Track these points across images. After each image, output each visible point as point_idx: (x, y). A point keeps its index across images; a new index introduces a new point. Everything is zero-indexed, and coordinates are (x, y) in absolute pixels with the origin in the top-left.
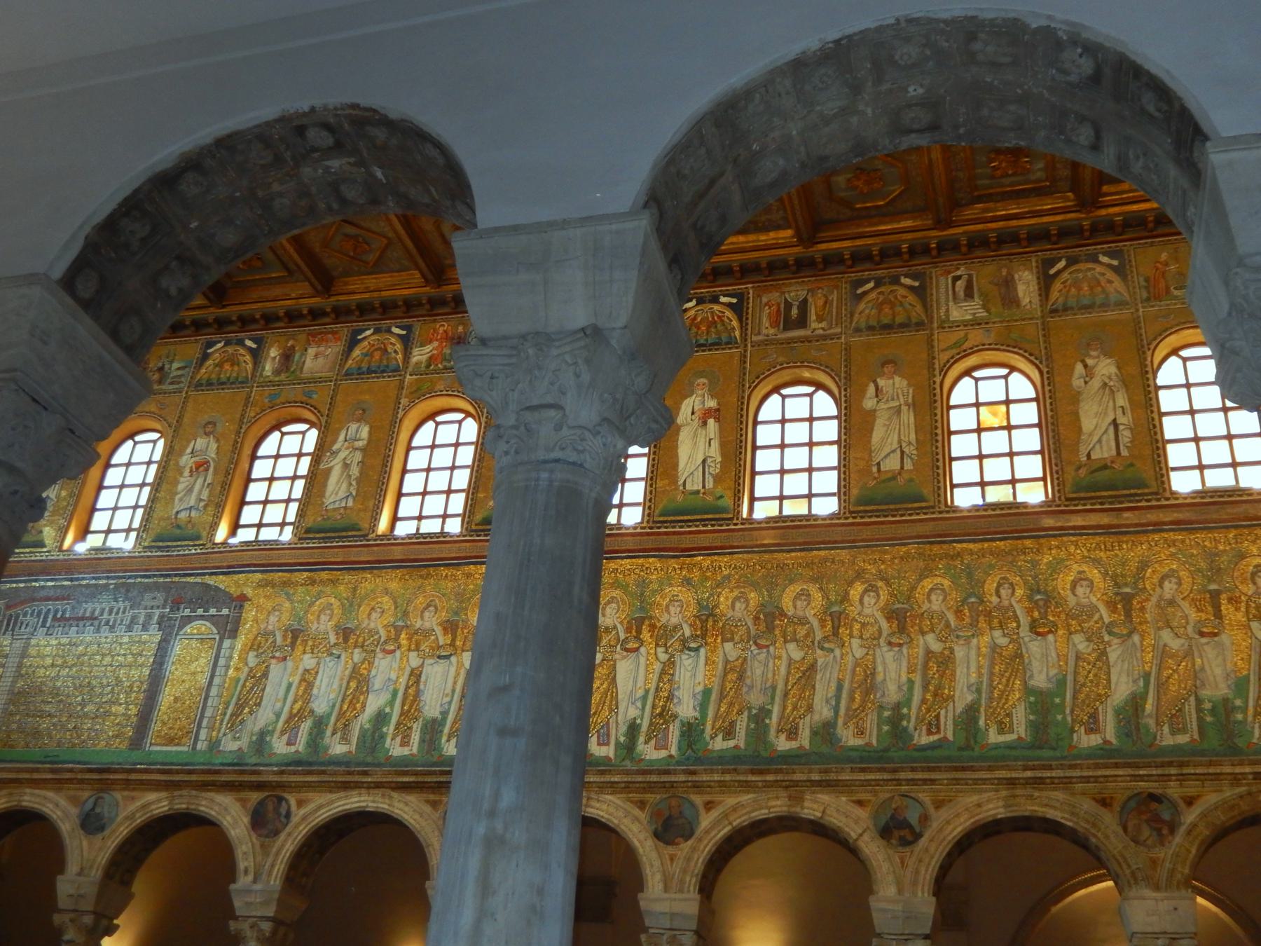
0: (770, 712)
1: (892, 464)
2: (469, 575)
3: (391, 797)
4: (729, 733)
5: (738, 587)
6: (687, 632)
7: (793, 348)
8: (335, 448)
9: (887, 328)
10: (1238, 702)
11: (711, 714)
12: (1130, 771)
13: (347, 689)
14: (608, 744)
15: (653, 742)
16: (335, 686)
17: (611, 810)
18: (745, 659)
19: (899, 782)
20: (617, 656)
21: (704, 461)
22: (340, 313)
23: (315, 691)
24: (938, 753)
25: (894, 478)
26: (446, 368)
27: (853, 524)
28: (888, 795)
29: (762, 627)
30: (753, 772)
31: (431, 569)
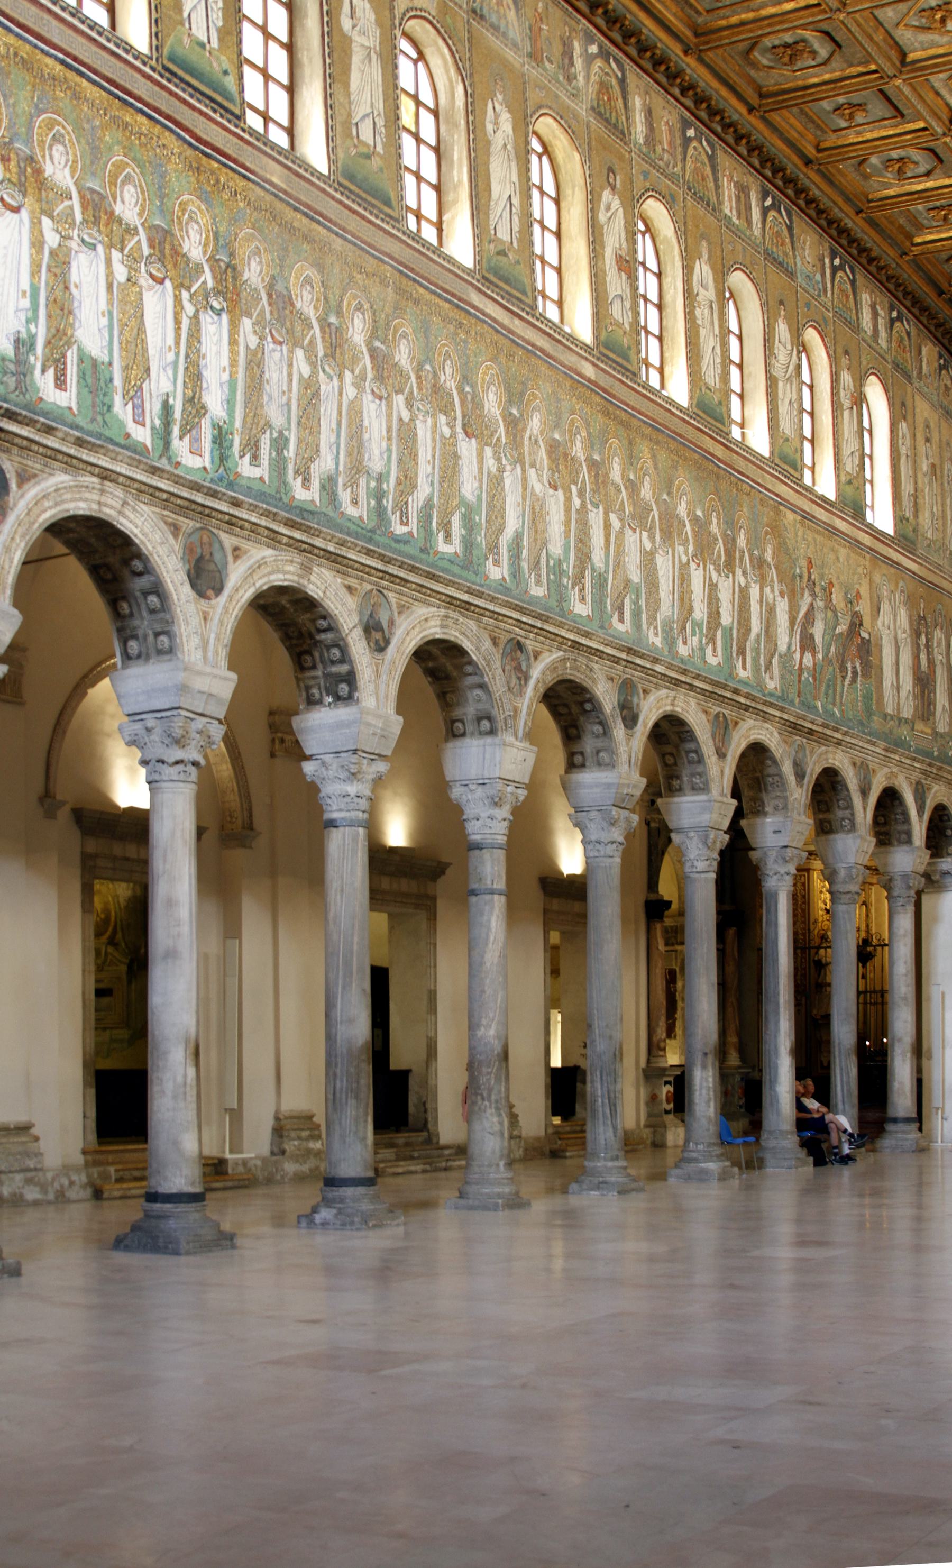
0: (287, 440)
6: (210, 284)
15: (187, 439)
17: (147, 528)
20: (142, 282)
25: (368, 157)
28: (369, 587)
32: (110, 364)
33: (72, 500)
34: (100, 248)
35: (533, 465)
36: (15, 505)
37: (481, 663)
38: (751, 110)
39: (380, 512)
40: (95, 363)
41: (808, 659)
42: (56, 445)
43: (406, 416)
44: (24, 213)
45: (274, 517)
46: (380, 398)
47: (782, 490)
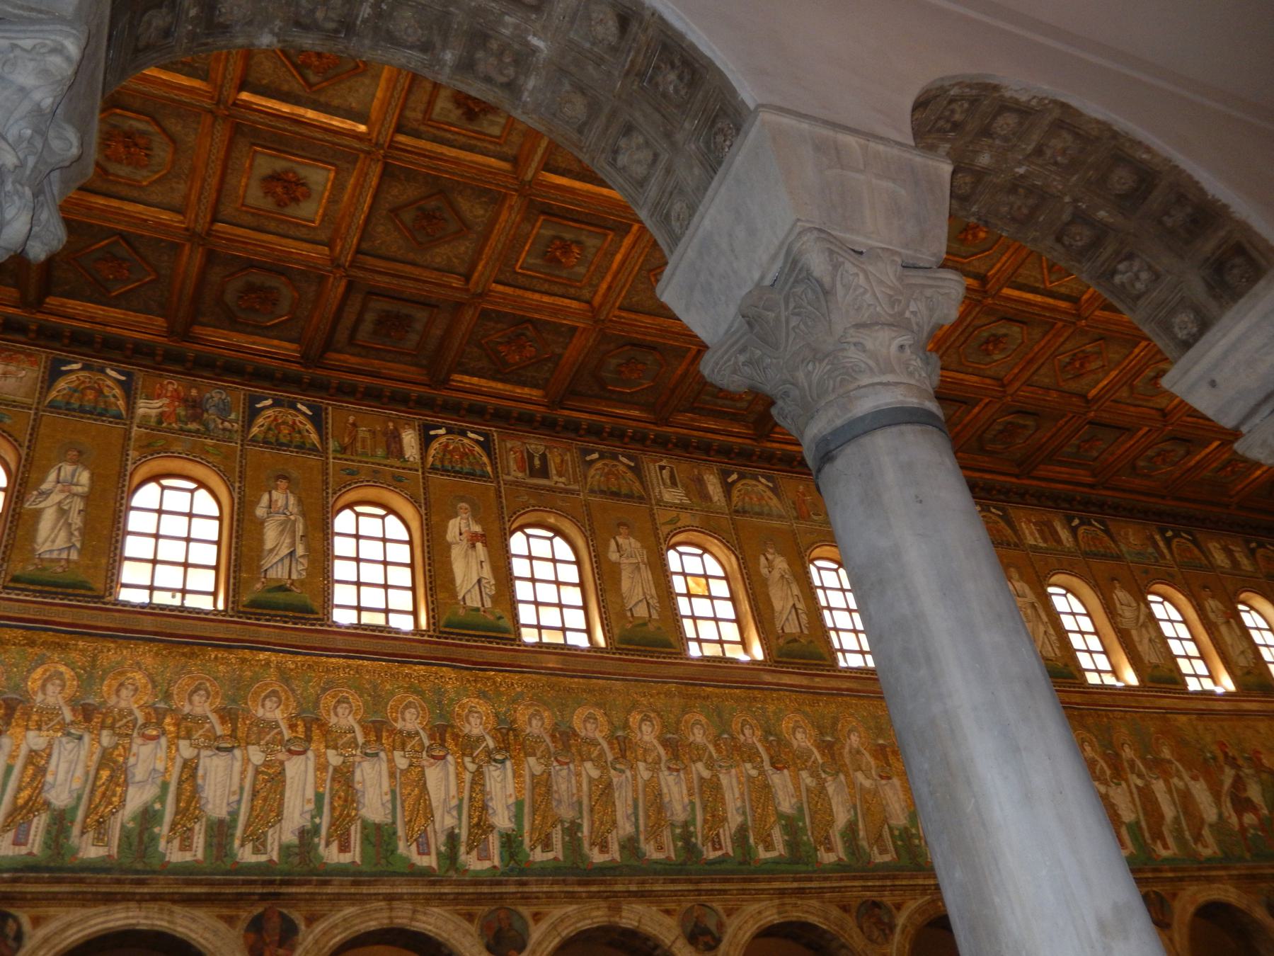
0: (580, 826)
1: (641, 611)
2: (243, 661)
3: (171, 912)
4: (547, 846)
5: (532, 705)
6: (491, 744)
7: (541, 495)
8: (44, 487)
9: (615, 495)
10: (914, 831)
11: (527, 827)
12: (861, 883)
13: (96, 778)
14: (429, 854)
15: (474, 853)
16: (79, 772)
18: (550, 774)
19: (699, 892)
20: (425, 763)
21: (479, 581)
22: (47, 335)
23: (49, 778)
24: (723, 866)
25: (645, 624)
26: (181, 429)
27: (619, 659)
28: (689, 905)
29: (560, 745)
30: (580, 883)
31: (196, 649)
32: (394, 823)
33: (362, 923)
34: (382, 754)
35: (859, 769)
36: (304, 940)
37: (833, 928)
38: (1017, 476)
39: (689, 848)
40: (378, 827)
41: (1249, 818)
42: (336, 891)
43: (706, 774)
44: (310, 754)
45: (565, 882)
46: (678, 770)
47: (1166, 702)
